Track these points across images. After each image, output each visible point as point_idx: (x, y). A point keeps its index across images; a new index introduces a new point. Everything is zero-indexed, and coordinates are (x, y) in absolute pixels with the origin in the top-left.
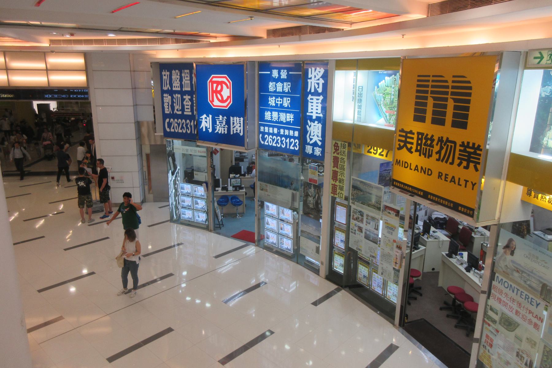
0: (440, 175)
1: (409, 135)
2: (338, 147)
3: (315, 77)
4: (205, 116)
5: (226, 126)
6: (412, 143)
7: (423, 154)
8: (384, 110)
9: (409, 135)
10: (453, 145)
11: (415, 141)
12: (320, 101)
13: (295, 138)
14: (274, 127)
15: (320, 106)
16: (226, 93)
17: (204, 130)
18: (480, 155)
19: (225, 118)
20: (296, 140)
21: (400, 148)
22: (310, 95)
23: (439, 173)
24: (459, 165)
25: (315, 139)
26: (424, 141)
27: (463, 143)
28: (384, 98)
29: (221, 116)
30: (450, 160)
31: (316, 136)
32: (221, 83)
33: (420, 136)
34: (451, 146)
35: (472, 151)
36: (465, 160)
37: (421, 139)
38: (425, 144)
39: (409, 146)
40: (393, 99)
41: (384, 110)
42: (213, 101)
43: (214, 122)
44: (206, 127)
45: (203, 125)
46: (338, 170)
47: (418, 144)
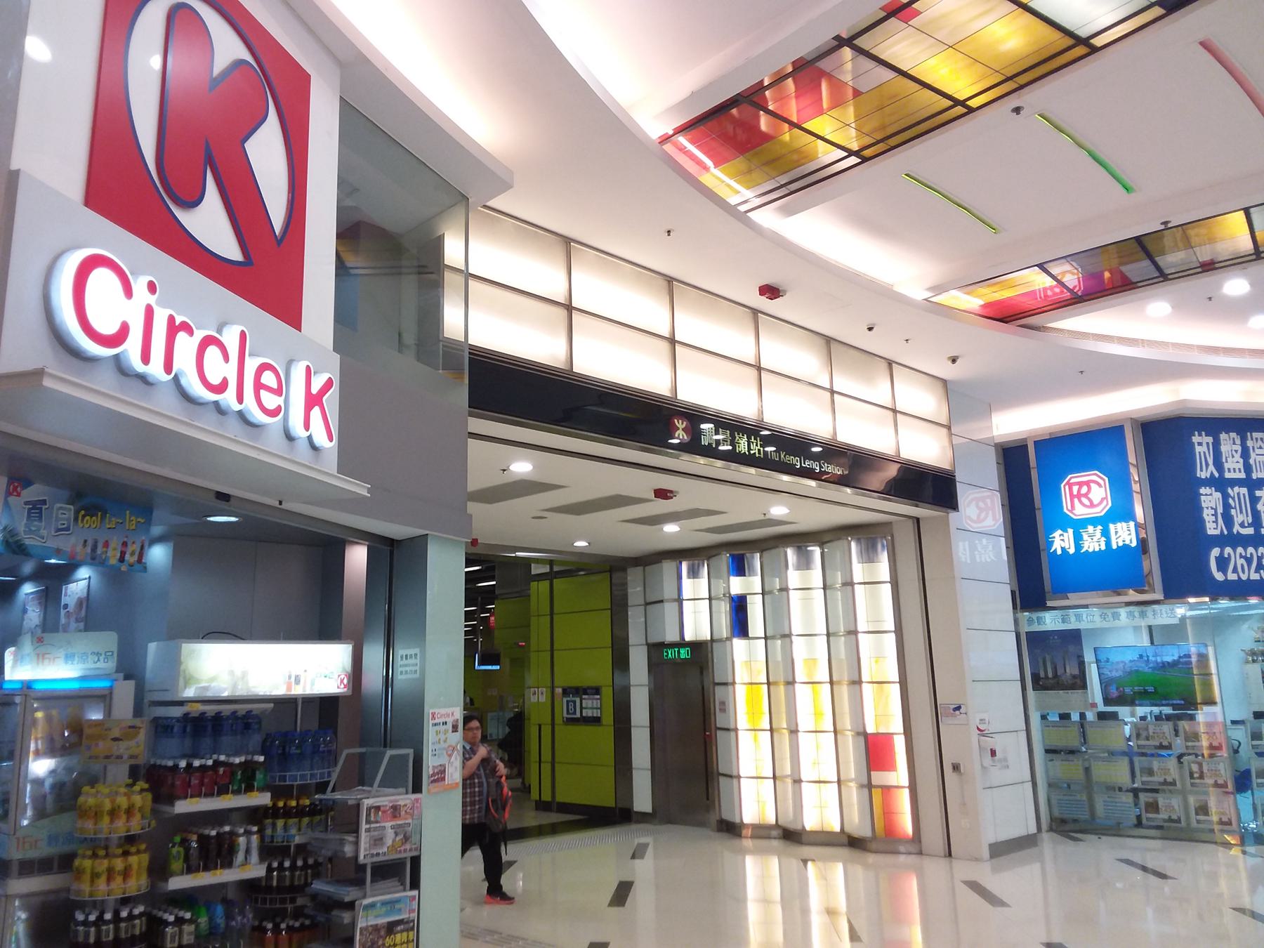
32: (1088, 483)
43: (1078, 539)
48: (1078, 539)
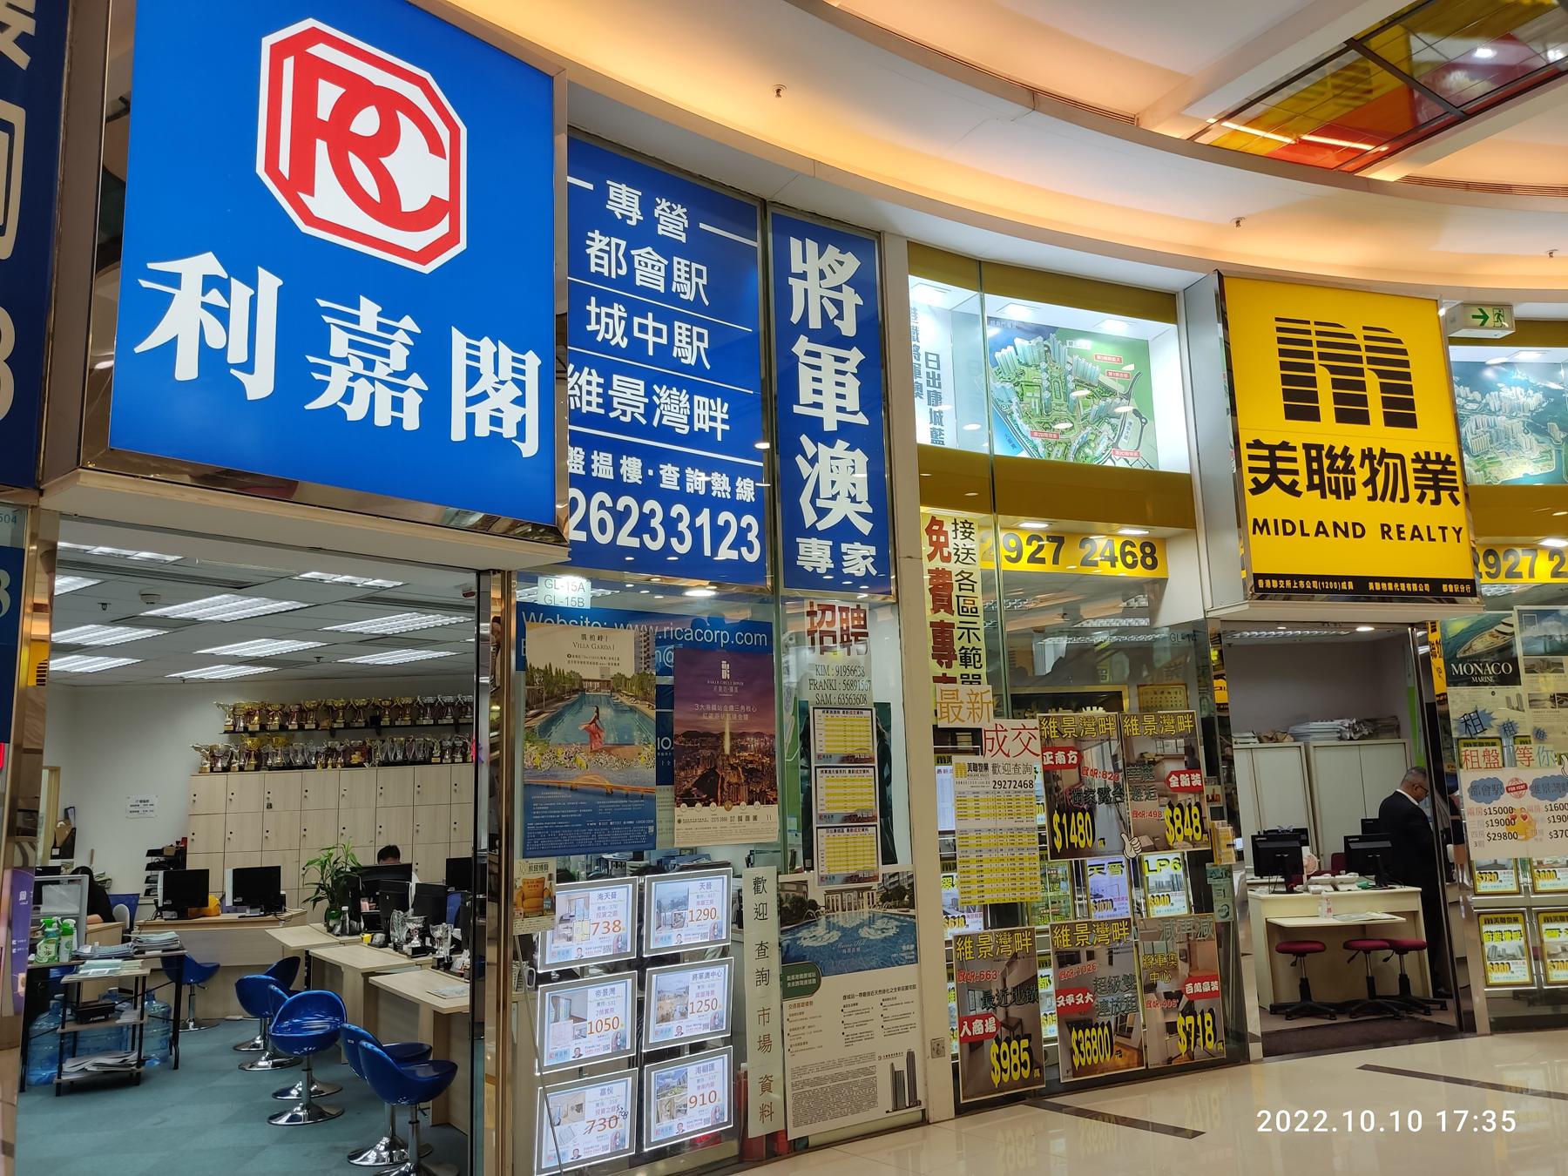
0: (1385, 531)
1: (1279, 453)
2: (945, 534)
3: (822, 276)
4: (207, 263)
5: (415, 381)
6: (1295, 472)
7: (1332, 492)
8: (1026, 429)
9: (1279, 453)
10: (1398, 461)
11: (1301, 465)
12: (851, 366)
13: (739, 508)
14: (619, 451)
15: (852, 386)
16: (419, 173)
17: (187, 367)
18: (1454, 473)
19: (408, 323)
20: (748, 519)
21: (1259, 488)
22: (803, 339)
23: (1383, 526)
24: (1421, 499)
25: (840, 510)
26: (1326, 462)
27: (1417, 454)
28: (1021, 397)
30: (1400, 494)
31: (843, 499)
32: (391, 104)
33: (1314, 453)
34: (1395, 465)
35: (1439, 467)
36: (1428, 487)
37: (1319, 459)
38: (1331, 470)
39: (1287, 479)
40: (1050, 399)
41: (1026, 429)
42: (302, 179)
43: (301, 338)
44: (211, 358)
45: (183, 325)
46: (955, 619)
47: (1311, 472)
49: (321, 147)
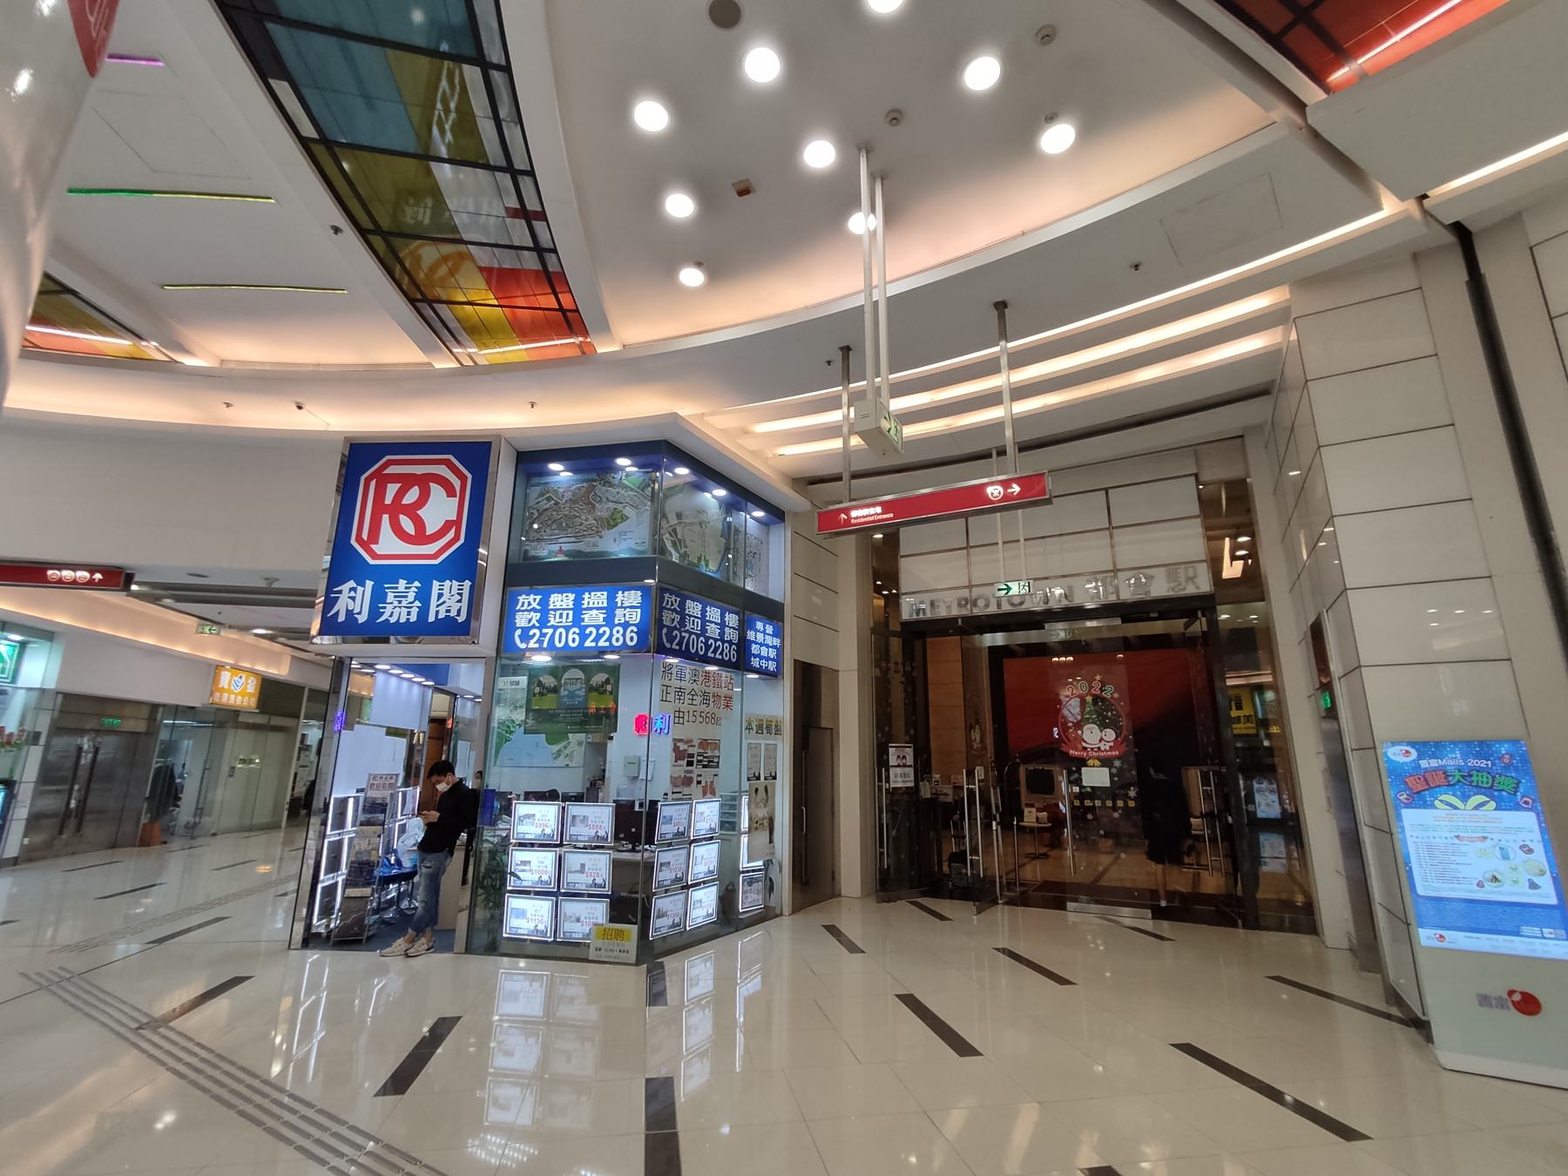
5: (418, 603)
17: (341, 618)
19: (417, 584)
29: (402, 583)
43: (378, 597)
44: (349, 613)
48: (378, 597)
49: (386, 517)
